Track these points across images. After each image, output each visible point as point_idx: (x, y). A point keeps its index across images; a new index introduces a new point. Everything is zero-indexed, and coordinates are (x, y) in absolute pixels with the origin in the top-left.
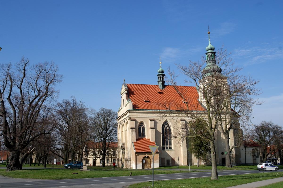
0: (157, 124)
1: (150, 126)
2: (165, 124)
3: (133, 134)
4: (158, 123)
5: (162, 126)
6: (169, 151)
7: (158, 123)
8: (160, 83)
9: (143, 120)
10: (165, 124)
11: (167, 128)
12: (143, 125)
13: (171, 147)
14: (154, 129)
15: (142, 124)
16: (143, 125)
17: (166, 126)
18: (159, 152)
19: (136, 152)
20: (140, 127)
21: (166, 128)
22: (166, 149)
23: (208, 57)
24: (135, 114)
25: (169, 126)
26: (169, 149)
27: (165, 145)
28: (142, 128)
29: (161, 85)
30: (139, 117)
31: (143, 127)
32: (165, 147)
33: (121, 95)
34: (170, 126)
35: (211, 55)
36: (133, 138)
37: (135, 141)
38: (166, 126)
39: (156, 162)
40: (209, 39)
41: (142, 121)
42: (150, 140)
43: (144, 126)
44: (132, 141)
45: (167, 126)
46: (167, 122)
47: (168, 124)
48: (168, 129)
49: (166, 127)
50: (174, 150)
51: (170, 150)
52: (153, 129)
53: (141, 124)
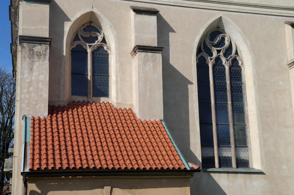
0: (171, 34)
1: (136, 37)
4: (173, 31)
5: (199, 51)
6: (239, 175)
7: (173, 31)
9: (95, 10)
11: (224, 60)
12: (100, 38)
13: (243, 155)
14: (159, 56)
15: (93, 34)
16: (100, 38)
18: (193, 171)
19: (27, 170)
20: (79, 46)
21: (218, 59)
22: (220, 166)
26: (238, 166)
27: (213, 146)
28: (89, 51)
31: (100, 48)
32: (213, 158)
34: (237, 53)
36: (29, 93)
37: (44, 113)
38: (219, 51)
41: (92, 14)
42: (136, 111)
43: (104, 41)
44: (26, 113)
45: (221, 54)
46: (223, 32)
47: (227, 43)
48: (227, 68)
49: (215, 54)
50: (261, 173)
51: (240, 170)
52: (150, 54)
53: (85, 30)
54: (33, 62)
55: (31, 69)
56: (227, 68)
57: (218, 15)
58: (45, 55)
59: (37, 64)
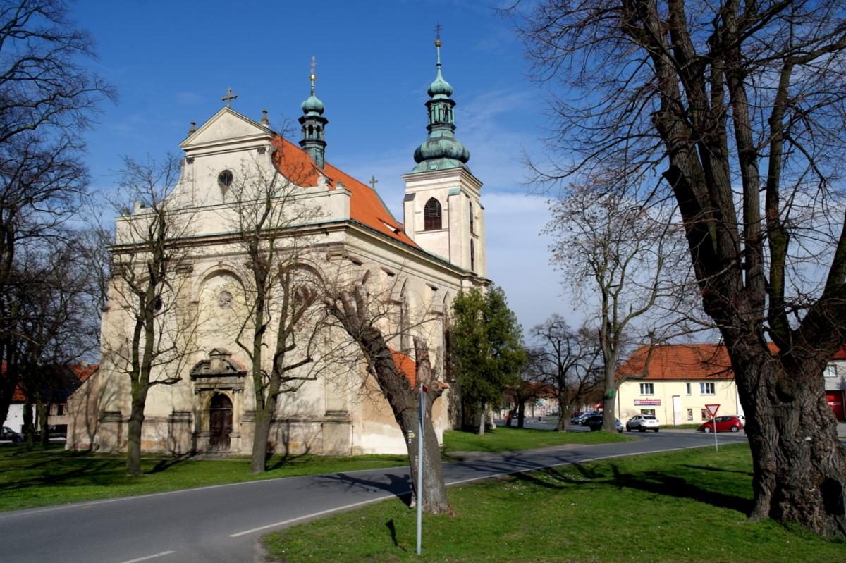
8: (317, 146)
23: (441, 111)
29: (319, 154)
33: (187, 151)
35: (449, 108)
40: (439, 63)
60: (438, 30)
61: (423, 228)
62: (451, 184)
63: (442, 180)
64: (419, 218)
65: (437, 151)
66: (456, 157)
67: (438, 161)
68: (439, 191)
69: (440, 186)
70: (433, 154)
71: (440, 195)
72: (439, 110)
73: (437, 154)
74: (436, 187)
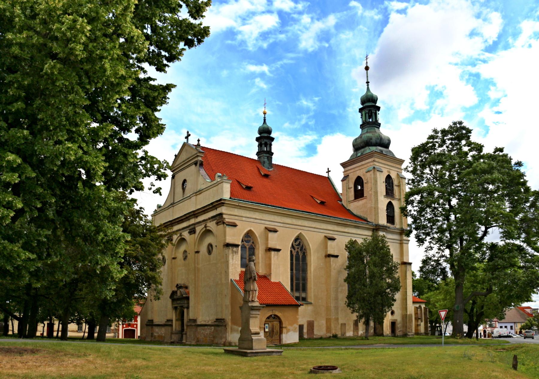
2: (295, 242)
3: (234, 261)
8: (265, 155)
9: (252, 229)
10: (295, 242)
17: (298, 248)
21: (298, 252)
23: (367, 115)
24: (236, 212)
25: (304, 248)
30: (244, 219)
34: (305, 249)
38: (298, 248)
39: (292, 330)
41: (250, 230)
45: (299, 250)
47: (301, 244)
48: (301, 256)
53: (245, 237)
54: (233, 255)
55: (233, 259)
56: (301, 256)
57: (300, 231)
58: (238, 252)
59: (235, 256)
60: (367, 59)
61: (353, 198)
62: (369, 165)
63: (363, 163)
64: (351, 192)
65: (361, 143)
66: (376, 145)
67: (363, 150)
68: (362, 170)
69: (362, 167)
70: (359, 146)
71: (360, 173)
72: (365, 114)
73: (362, 145)
74: (360, 168)
